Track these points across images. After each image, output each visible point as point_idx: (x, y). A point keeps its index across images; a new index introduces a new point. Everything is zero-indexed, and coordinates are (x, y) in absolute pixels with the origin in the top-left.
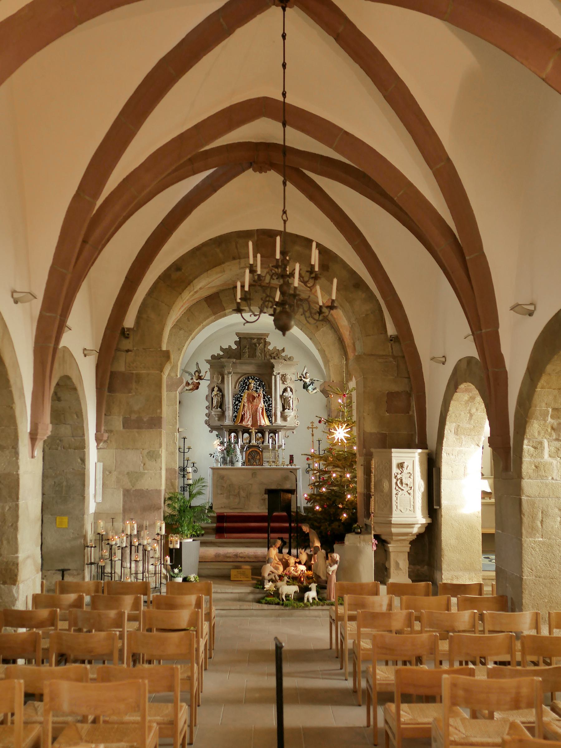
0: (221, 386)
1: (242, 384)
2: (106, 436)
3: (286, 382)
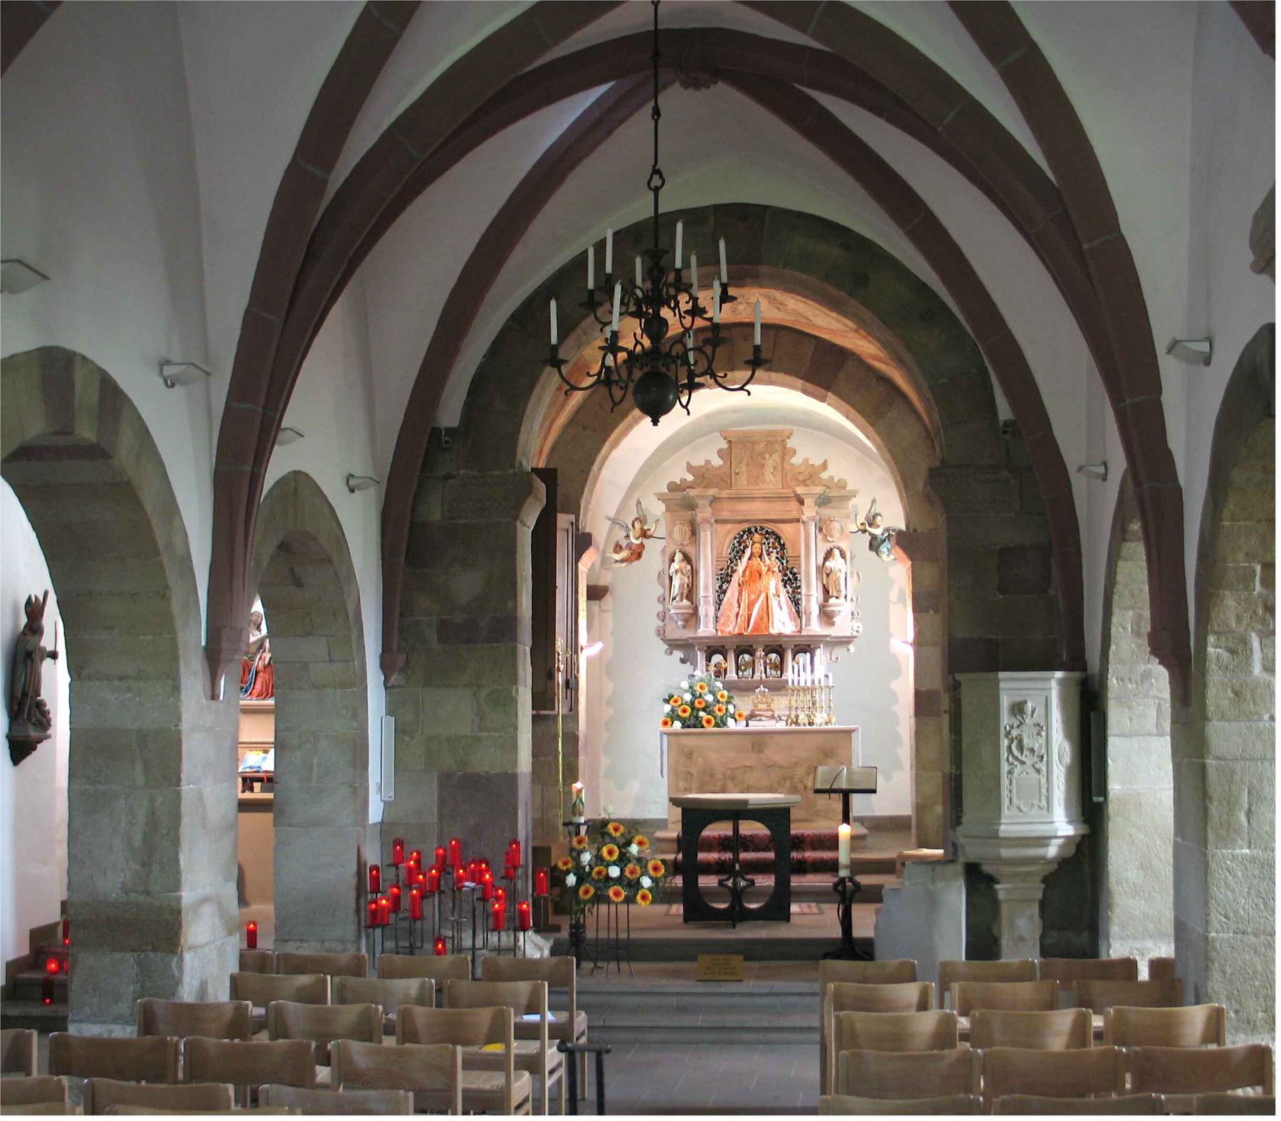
0: (690, 550)
1: (736, 544)
2: (401, 659)
3: (831, 536)
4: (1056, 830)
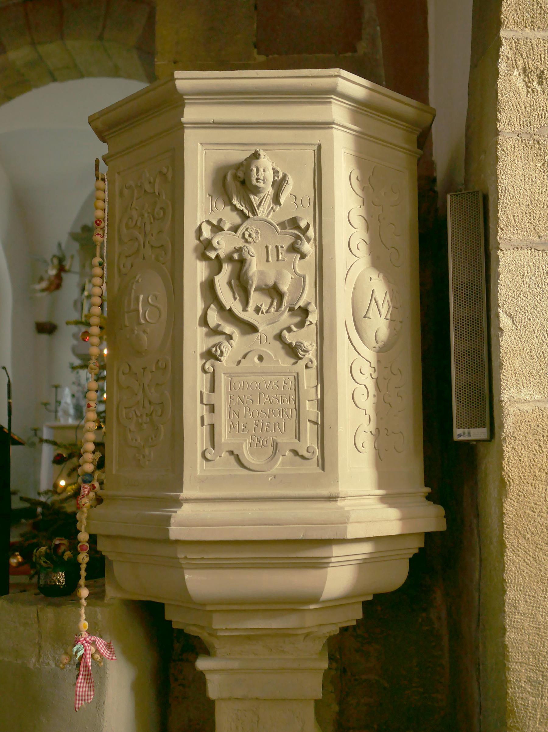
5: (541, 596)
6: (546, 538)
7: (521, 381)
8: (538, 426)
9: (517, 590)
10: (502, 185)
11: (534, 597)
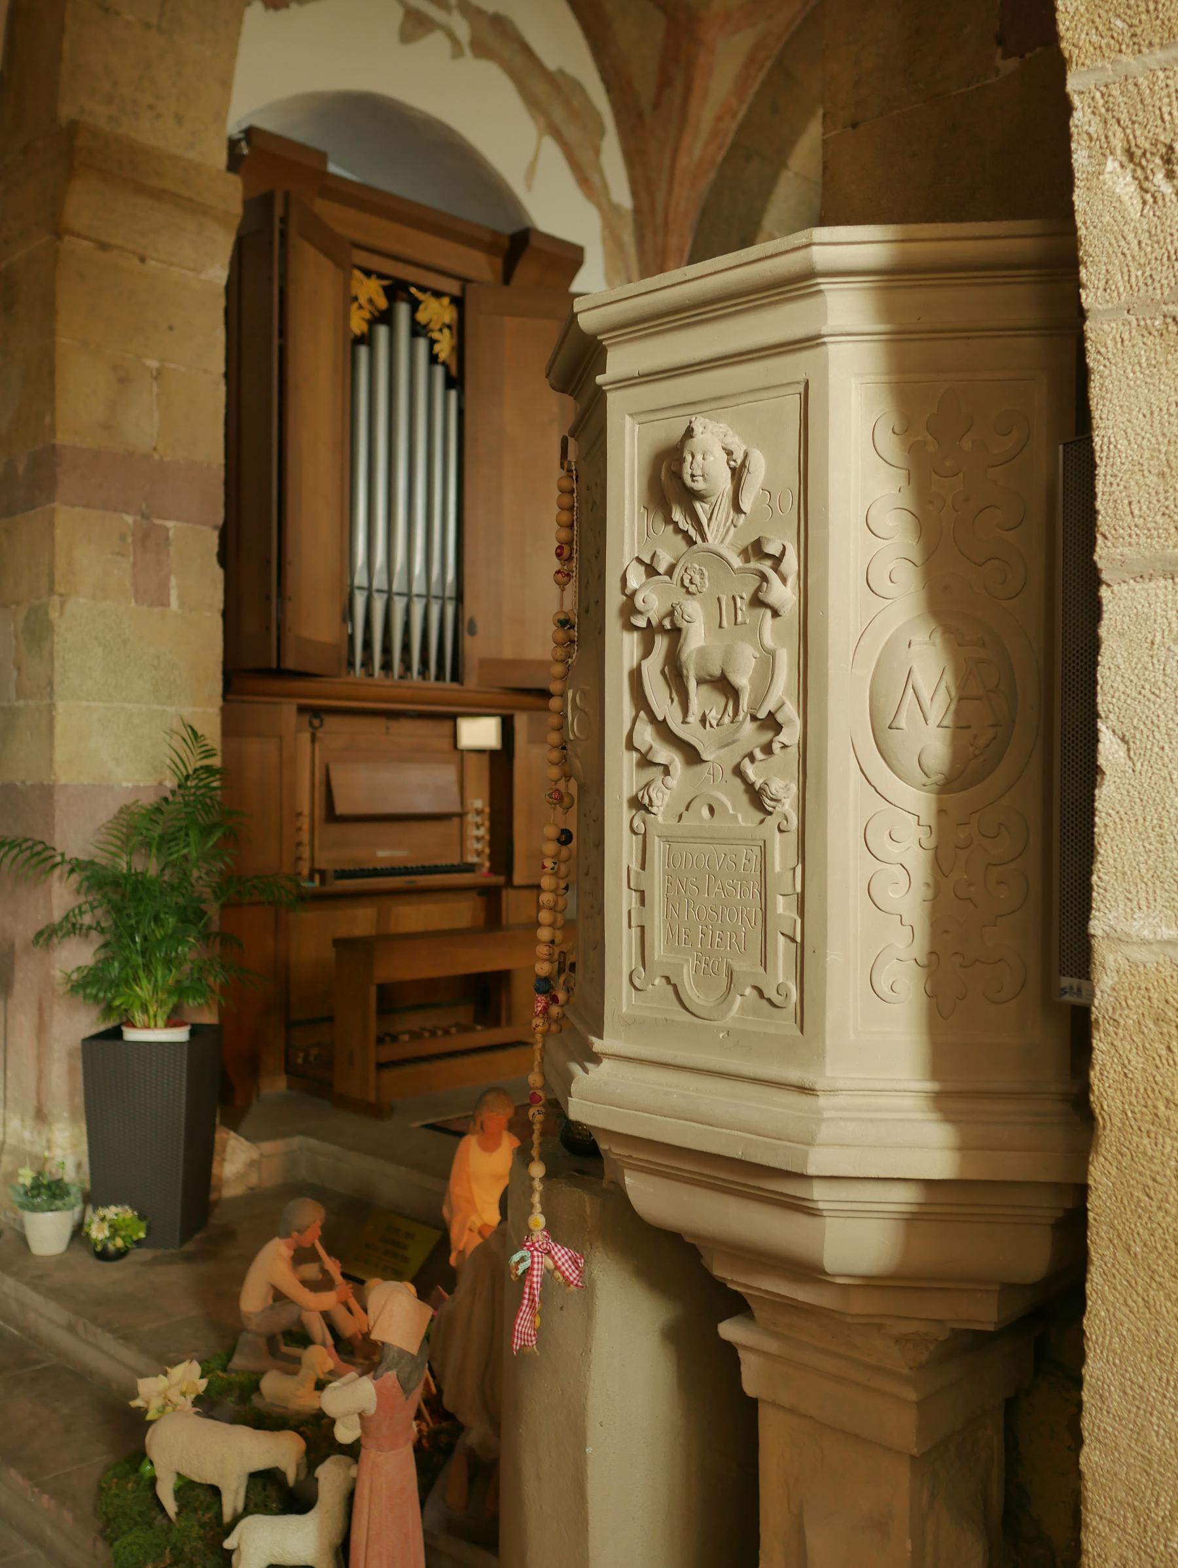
4: (810, 1142)
5: (1156, 1391)
6: (1172, 1263)
7: (1134, 892)
8: (1167, 1002)
9: (1108, 1362)
10: (1103, 432)
11: (1141, 1387)
